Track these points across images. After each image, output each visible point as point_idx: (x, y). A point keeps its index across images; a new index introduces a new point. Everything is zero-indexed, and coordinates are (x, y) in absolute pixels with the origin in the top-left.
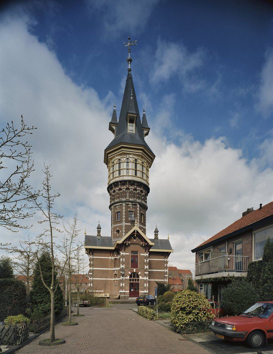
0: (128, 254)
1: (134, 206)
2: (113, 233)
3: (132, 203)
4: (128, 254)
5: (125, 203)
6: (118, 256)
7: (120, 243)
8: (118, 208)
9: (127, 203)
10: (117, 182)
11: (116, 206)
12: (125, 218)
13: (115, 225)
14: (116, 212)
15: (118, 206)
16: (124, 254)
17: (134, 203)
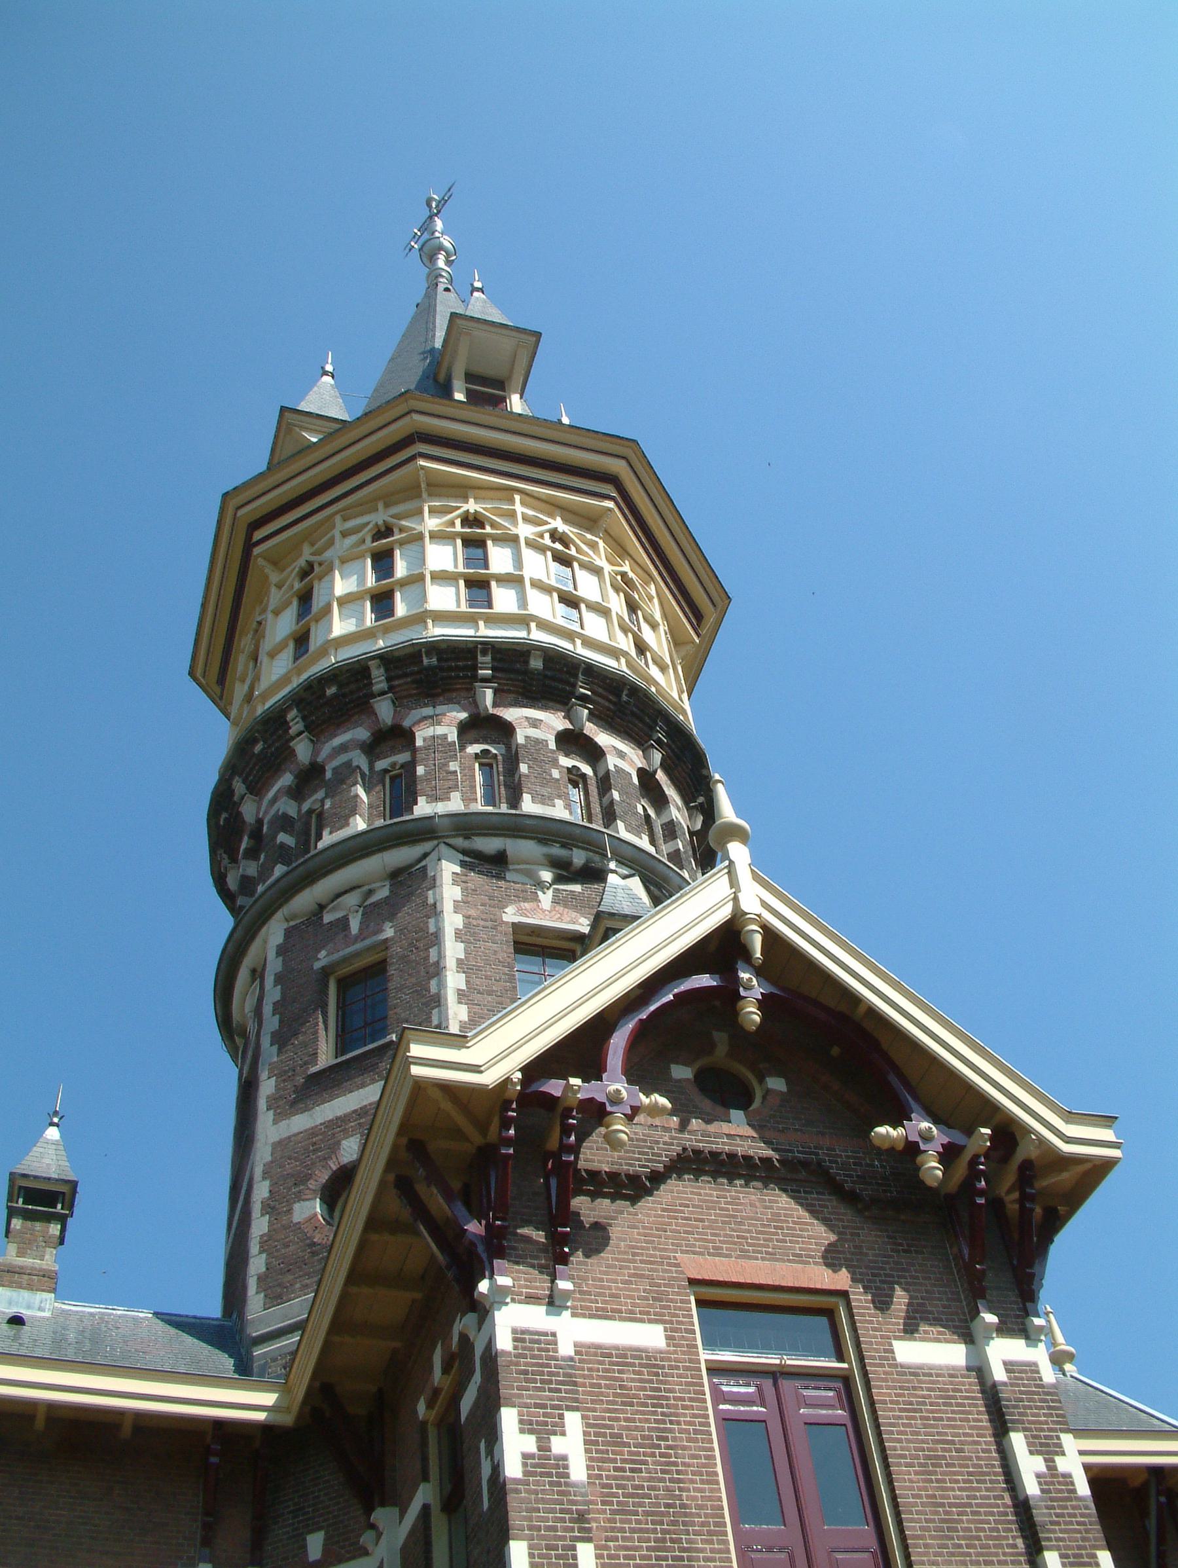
0: (649, 1336)
1: (577, 888)
2: (260, 1225)
3: (557, 851)
4: (649, 1336)
5: (459, 842)
6: (382, 1516)
7: (489, 1078)
8: (355, 925)
9: (489, 845)
10: (357, 672)
11: (322, 907)
12: (461, 996)
13: (300, 1122)
14: (326, 972)
15: (352, 899)
16: (572, 1332)
17: (579, 858)
